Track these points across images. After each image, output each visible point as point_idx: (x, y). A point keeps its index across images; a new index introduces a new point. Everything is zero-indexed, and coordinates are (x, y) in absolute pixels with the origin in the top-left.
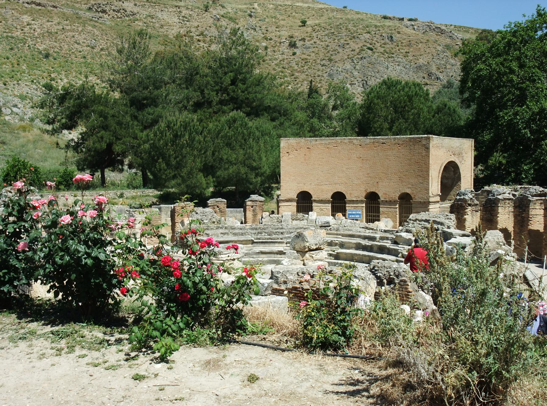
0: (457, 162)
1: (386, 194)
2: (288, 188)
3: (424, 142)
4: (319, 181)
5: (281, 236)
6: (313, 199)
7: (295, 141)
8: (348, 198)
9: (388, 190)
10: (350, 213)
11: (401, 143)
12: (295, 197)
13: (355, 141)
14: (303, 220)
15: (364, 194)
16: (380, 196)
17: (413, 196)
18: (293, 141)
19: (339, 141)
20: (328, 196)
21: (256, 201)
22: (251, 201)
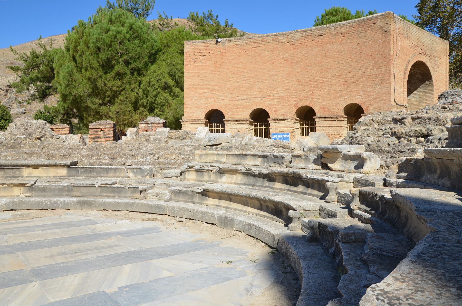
0: (428, 64)
1: (324, 108)
2: (194, 106)
3: (380, 23)
4: (233, 95)
5: (129, 161)
6: (226, 118)
7: (203, 44)
8: (272, 115)
9: (329, 102)
10: (274, 137)
11: (344, 30)
12: (203, 117)
13: (281, 38)
14: (185, 138)
15: (295, 110)
16: (316, 111)
17: (364, 108)
18: (201, 44)
19: (260, 39)
20: (246, 115)
21: (152, 123)
22: (145, 123)
